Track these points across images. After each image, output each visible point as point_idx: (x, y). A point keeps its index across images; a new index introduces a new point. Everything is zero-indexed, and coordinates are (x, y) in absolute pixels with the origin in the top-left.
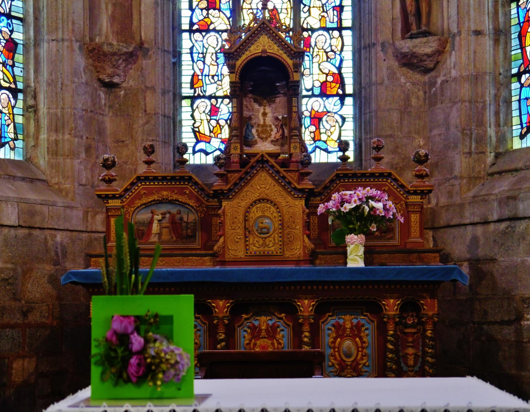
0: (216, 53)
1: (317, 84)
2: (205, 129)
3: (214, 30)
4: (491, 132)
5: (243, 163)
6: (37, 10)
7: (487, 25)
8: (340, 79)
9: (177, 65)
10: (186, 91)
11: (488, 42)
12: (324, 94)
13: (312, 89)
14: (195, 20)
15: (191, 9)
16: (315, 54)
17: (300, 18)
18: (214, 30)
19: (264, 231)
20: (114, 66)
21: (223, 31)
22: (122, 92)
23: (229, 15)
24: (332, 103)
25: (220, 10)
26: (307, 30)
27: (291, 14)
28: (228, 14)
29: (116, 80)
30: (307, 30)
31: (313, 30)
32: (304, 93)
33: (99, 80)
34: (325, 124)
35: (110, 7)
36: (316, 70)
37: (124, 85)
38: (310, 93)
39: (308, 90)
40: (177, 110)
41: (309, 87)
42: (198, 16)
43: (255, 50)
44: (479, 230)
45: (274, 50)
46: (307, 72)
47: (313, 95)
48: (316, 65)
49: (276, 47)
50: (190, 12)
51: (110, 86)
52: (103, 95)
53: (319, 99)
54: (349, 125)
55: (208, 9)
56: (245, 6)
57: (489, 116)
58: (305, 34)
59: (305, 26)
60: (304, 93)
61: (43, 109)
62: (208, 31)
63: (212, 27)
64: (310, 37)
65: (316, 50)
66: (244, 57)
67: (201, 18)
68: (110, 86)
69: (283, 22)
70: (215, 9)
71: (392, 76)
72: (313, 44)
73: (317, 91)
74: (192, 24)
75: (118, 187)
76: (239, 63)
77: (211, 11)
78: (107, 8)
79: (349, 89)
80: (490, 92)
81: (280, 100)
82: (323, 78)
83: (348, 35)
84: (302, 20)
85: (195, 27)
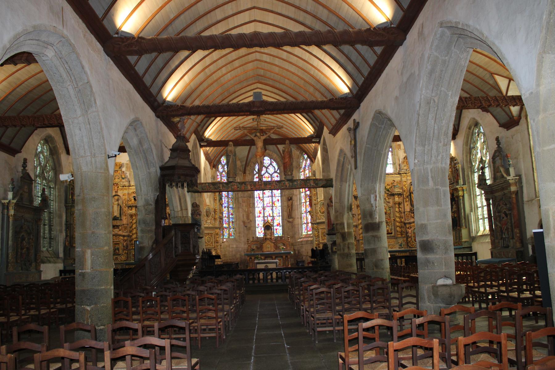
2: (260, 232)
4: (300, 232)
5: (266, 239)
6: (236, 217)
7: (299, 217)
8: (279, 224)
9: (255, 222)
10: (257, 226)
11: (299, 220)
12: (277, 225)
19: (268, 248)
24: (278, 227)
34: (277, 230)
40: (256, 229)
42: (258, 215)
43: (266, 225)
44: (298, 246)
45: (269, 224)
54: (281, 230)
57: (300, 229)
61: (237, 231)
71: (287, 224)
75: (250, 242)
79: (281, 225)
80: (300, 226)
81: (270, 230)
83: (281, 217)
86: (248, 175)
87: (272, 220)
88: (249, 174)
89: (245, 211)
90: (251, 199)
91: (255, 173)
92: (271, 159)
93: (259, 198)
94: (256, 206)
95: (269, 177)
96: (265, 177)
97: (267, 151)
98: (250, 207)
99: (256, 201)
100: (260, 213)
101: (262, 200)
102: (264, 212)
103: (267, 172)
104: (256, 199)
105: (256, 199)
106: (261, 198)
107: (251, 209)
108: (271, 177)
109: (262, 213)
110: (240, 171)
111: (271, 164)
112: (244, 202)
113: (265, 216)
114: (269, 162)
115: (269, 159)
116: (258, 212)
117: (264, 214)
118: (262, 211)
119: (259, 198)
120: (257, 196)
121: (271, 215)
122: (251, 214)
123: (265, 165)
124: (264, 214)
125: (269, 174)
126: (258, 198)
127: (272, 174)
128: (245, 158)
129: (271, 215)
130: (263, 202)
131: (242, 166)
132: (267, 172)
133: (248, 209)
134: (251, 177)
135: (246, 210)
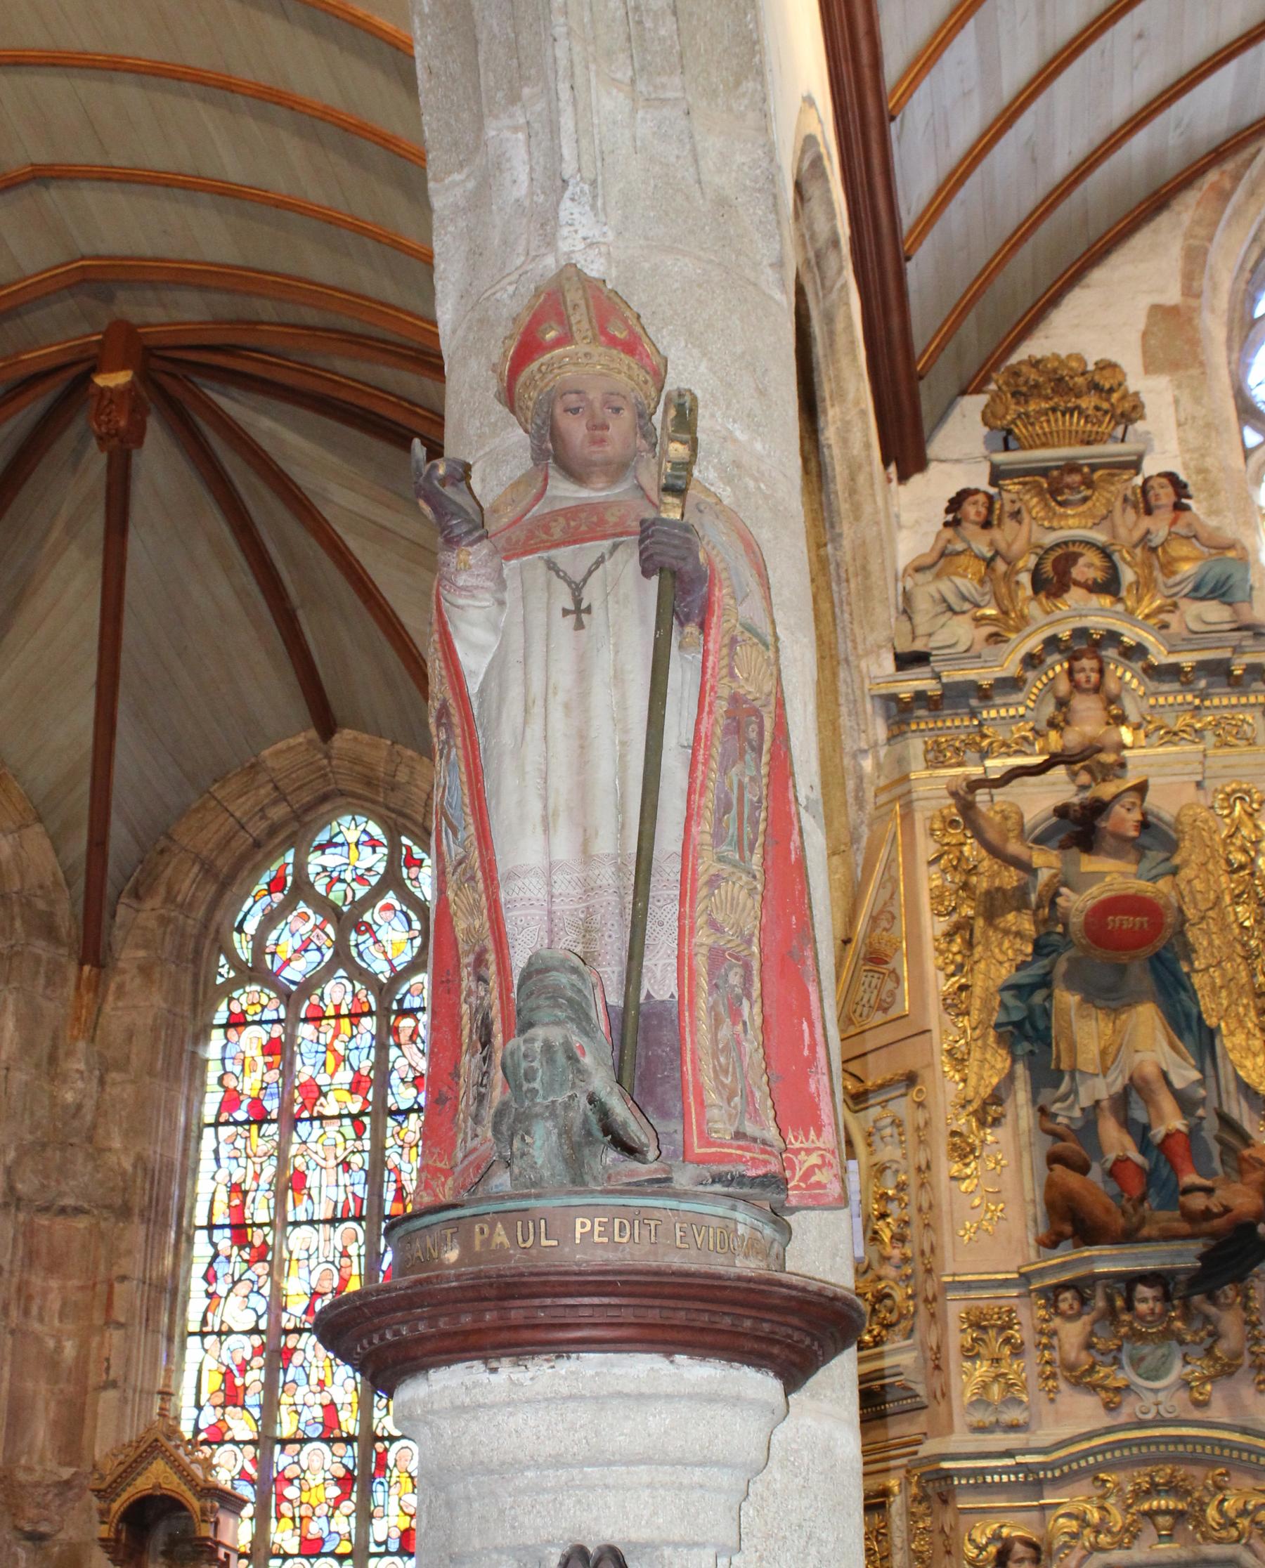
0: (233, 1479)
1: (396, 1534)
3: (233, 1441)
13: (385, 1543)
14: (202, 1425)
15: (199, 1407)
16: (393, 1480)
17: (371, 1418)
18: (233, 1441)
20: (38, 1505)
21: (246, 1443)
22: (56, 1549)
23: (257, 1416)
25: (243, 1407)
26: (382, 1439)
27: (356, 1414)
28: (256, 1413)
29: (44, 1528)
30: (382, 1439)
31: (392, 1439)
32: (373, 1548)
33: (16, 1528)
35: (53, 1404)
36: (393, 1509)
37: (61, 1536)
38: (382, 1549)
39: (378, 1544)
41: (381, 1538)
42: (209, 1417)
45: (173, 1484)
46: (378, 1512)
47: (388, 1553)
48: (394, 1500)
49: (175, 1479)
50: (196, 1412)
51: (36, 1538)
52: (22, 1554)
53: (396, 1559)
55: (223, 1406)
56: (285, 1399)
58: (379, 1446)
59: (379, 1433)
60: (373, 1548)
62: (221, 1443)
63: (228, 1436)
64: (386, 1450)
65: (395, 1473)
66: (125, 1496)
67: (213, 1420)
68: (36, 1538)
69: (344, 1427)
70: (235, 1406)
72: (391, 1463)
73: (394, 1546)
74: (197, 1431)
76: (118, 1506)
77: (230, 1409)
78: (46, 1408)
82: (404, 1523)
84: (375, 1422)
85: (202, 1436)
86: (133, 982)
87: (345, 1482)
88: (145, 970)
89: (52, 1363)
90: (136, 1232)
91: (225, 971)
92: (393, 833)
93: (239, 1230)
94: (194, 1326)
95: (354, 1017)
96: (316, 1018)
97: (344, 739)
98: (109, 1322)
99: (199, 1269)
100: (232, 1396)
101: (261, 1254)
102: (270, 1387)
103: (342, 957)
104: (201, 1247)
105: (201, 1237)
106: (256, 1237)
107: (116, 1336)
108: (383, 1013)
109: (253, 1398)
110: (49, 931)
111: (391, 880)
112: (54, 1267)
113: (286, 1427)
114: (375, 861)
115: (376, 830)
116: (213, 1382)
117: (270, 1408)
118: (255, 1377)
119: (239, 1230)
120: (221, 1218)
121: (349, 1422)
122: (111, 1395)
123: (336, 895)
124: (270, 1408)
125: (367, 978)
126: (223, 1238)
127: (399, 977)
128: (85, 786)
129: (349, 1422)
130: (277, 1272)
131: (68, 872)
132: (342, 957)
133: (84, 1345)
134: (158, 1000)
135: (69, 1349)
